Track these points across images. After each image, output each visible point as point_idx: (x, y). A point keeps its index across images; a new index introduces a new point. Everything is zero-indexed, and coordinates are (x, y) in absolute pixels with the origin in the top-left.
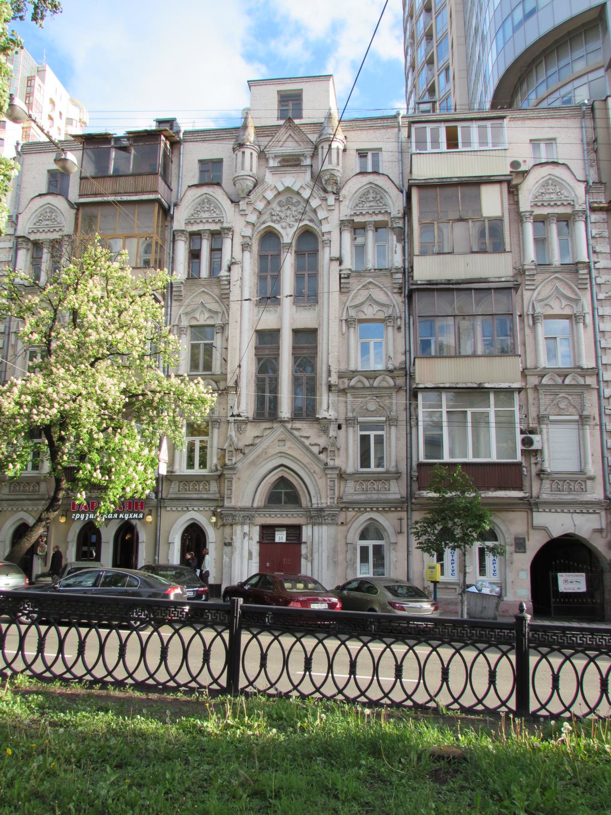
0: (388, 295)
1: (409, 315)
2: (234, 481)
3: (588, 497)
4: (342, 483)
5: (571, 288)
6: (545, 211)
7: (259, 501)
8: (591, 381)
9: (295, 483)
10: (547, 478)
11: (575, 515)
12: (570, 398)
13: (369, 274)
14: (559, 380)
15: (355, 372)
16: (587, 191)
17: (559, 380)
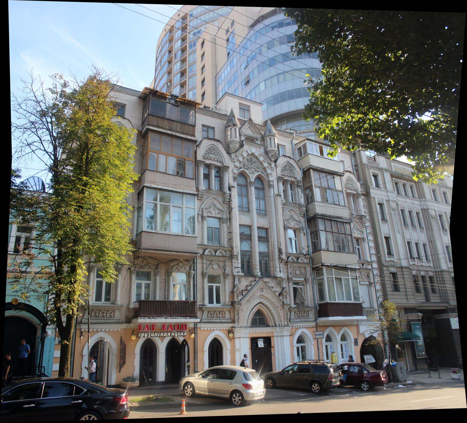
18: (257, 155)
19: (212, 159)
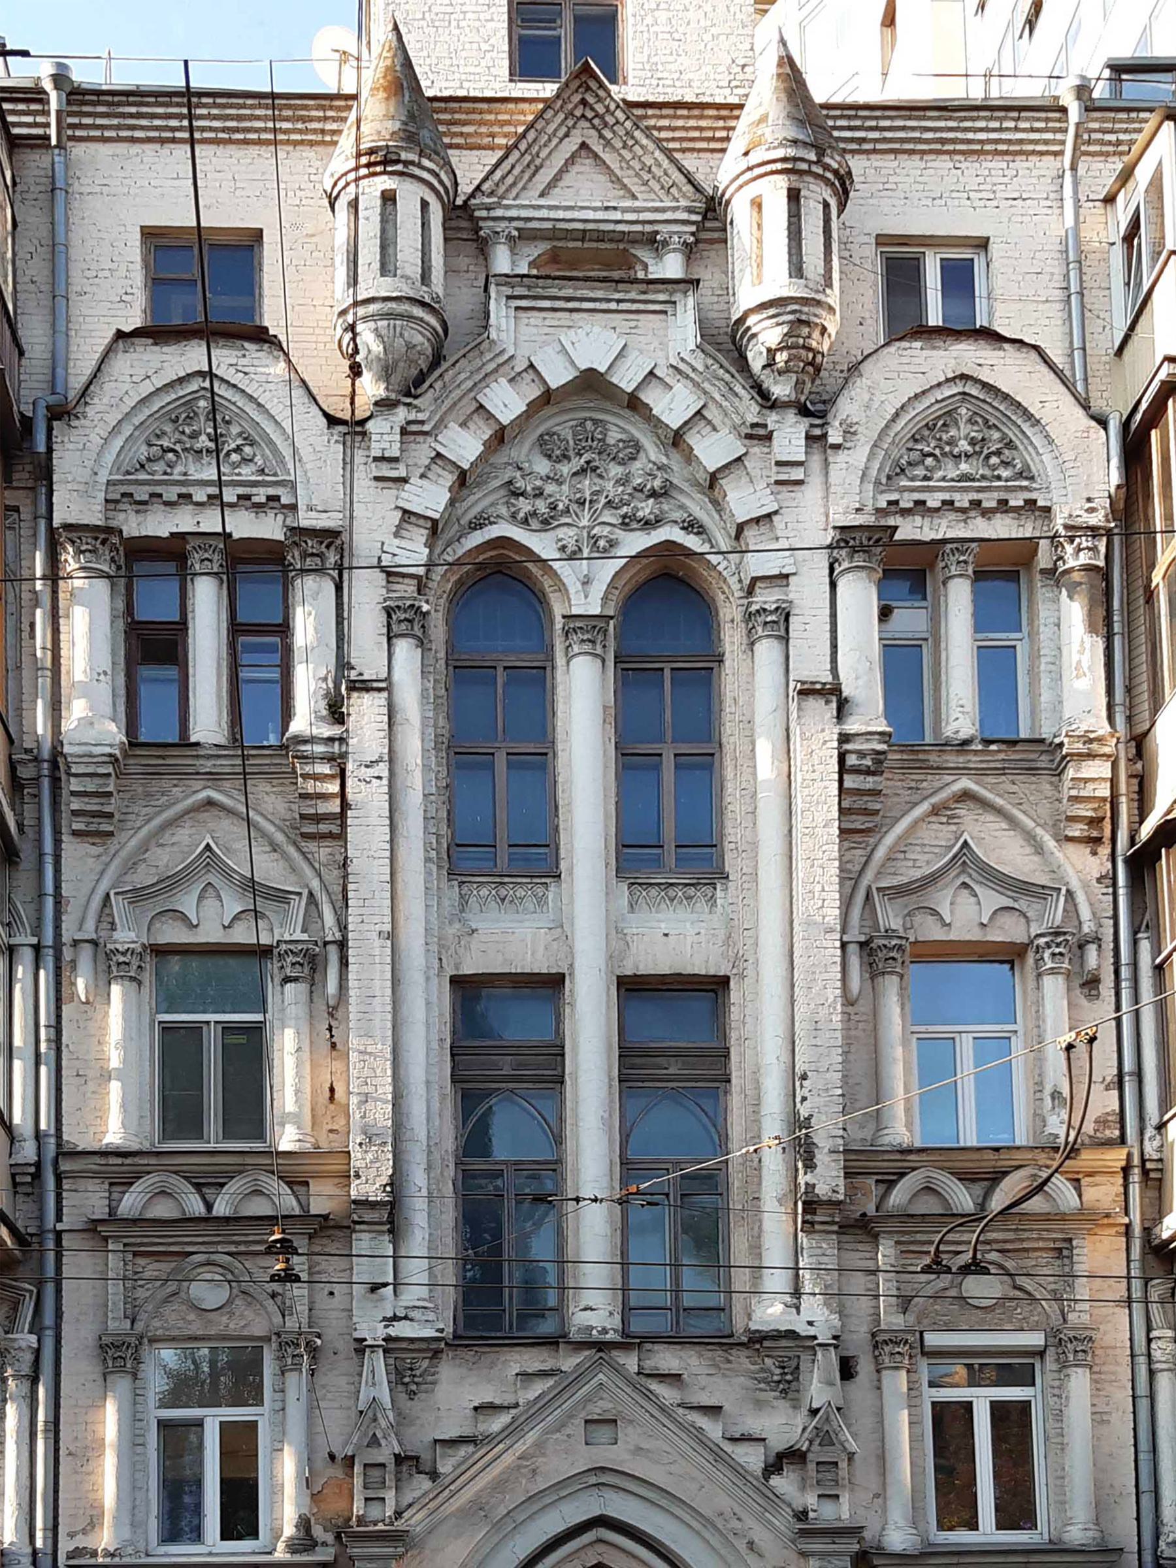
0: (1039, 849)
1: (1135, 932)
13: (953, 760)
18: (626, 379)
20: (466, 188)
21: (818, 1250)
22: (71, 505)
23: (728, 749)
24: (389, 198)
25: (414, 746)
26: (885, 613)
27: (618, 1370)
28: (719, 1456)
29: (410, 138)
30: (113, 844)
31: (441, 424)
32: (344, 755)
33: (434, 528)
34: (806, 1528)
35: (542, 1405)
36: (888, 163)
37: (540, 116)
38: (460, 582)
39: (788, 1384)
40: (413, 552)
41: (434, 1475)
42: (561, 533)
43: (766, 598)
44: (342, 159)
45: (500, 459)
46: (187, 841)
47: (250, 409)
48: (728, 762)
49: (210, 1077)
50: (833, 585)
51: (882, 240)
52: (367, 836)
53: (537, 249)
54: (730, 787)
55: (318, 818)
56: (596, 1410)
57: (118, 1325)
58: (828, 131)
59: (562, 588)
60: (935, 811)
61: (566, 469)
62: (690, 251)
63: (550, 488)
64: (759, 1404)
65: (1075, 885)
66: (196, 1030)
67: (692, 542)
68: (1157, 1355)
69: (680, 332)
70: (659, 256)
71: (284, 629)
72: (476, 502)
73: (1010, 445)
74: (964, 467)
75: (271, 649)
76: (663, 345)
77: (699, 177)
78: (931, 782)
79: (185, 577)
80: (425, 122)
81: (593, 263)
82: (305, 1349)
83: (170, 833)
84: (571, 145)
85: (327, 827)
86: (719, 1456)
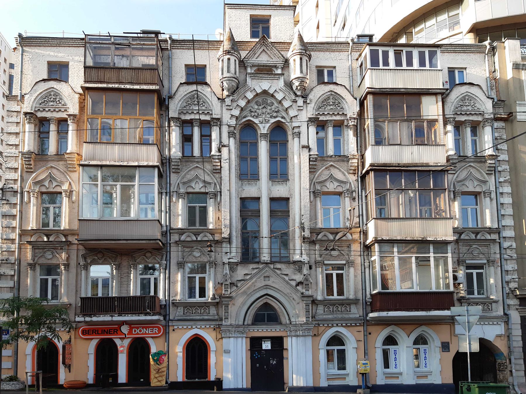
0: (345, 175)
1: (362, 190)
2: (230, 306)
3: (494, 314)
4: (314, 307)
5: (481, 173)
6: (463, 118)
7: (249, 320)
8: (494, 236)
9: (276, 307)
10: (466, 302)
11: (484, 326)
12: (480, 248)
13: (329, 159)
14: (473, 236)
15: (321, 230)
16: (493, 106)
17: (473, 236)
18: (271, 91)
19: (195, 112)
20: (243, 57)
21: (305, 246)
22: (173, 113)
23: (289, 157)
24: (229, 59)
25: (233, 157)
26: (317, 133)
27: (270, 268)
28: (288, 283)
29: (233, 48)
30: (180, 174)
31: (238, 99)
32: (221, 158)
33: (237, 118)
34: (303, 296)
35: (256, 274)
36: (318, 53)
37: (256, 44)
38: (241, 127)
39: (300, 270)
40: (233, 122)
41: (237, 286)
42: (260, 119)
43: (296, 130)
44: (220, 52)
45: (249, 105)
46: (193, 173)
47: (204, 97)
48: (289, 160)
49: (197, 216)
50: (308, 128)
51: (317, 67)
52: (225, 173)
53: (255, 68)
54: (290, 164)
55: (216, 170)
56: (266, 275)
57: (180, 260)
58: (307, 47)
59: (260, 128)
60: (326, 168)
61: (260, 107)
62: (282, 69)
63: (258, 111)
64: (295, 274)
65: (351, 181)
66: (194, 207)
67: (283, 120)
68: (366, 265)
69: (281, 83)
70: (277, 70)
71: (210, 136)
72: (245, 113)
73: (339, 103)
74: (331, 107)
75: (207, 139)
76: (278, 85)
77: (284, 55)
78: (325, 163)
79: (192, 126)
80: (235, 46)
81: (265, 71)
82: (214, 264)
83: (190, 172)
84: (261, 50)
85: (218, 171)
86: (288, 283)
